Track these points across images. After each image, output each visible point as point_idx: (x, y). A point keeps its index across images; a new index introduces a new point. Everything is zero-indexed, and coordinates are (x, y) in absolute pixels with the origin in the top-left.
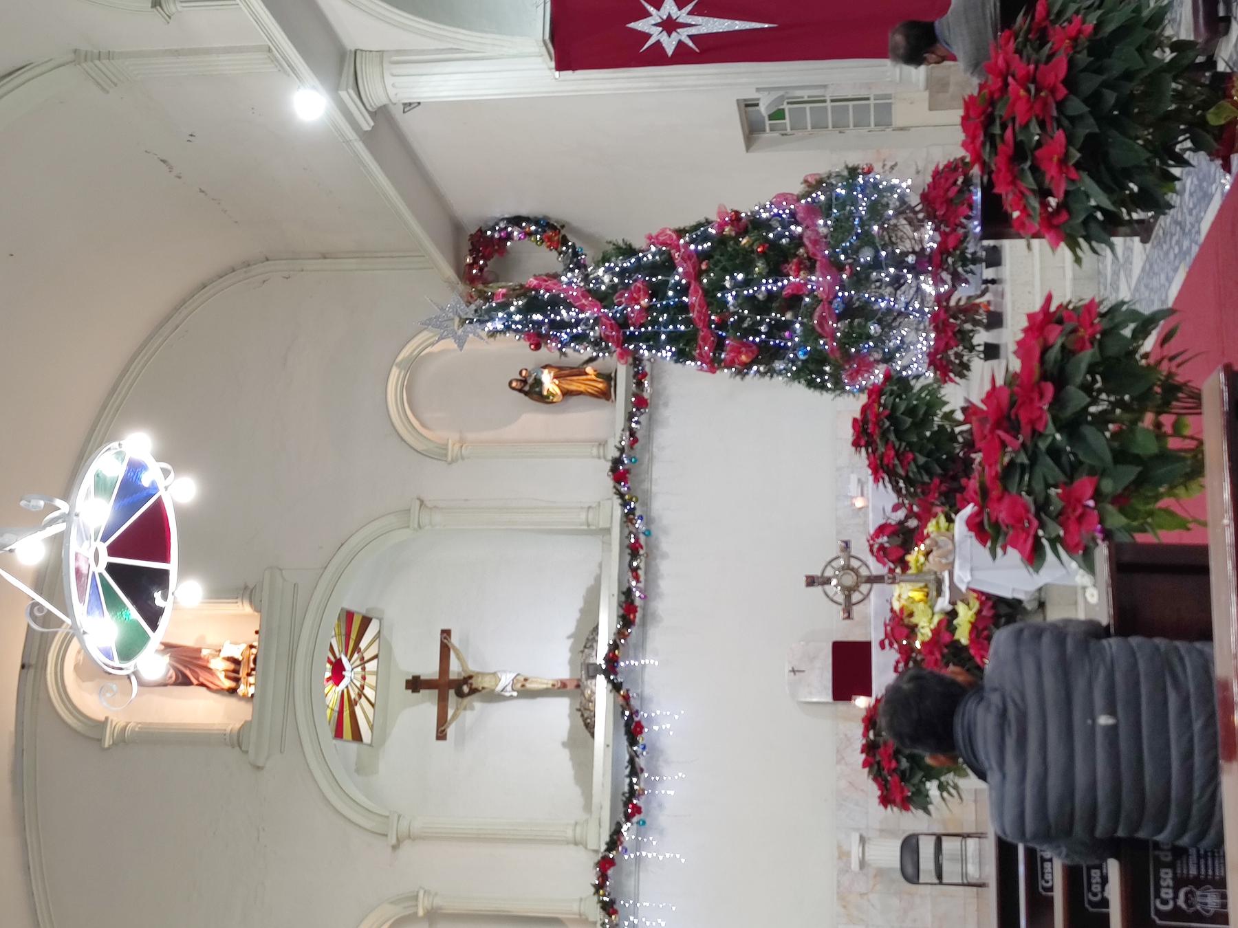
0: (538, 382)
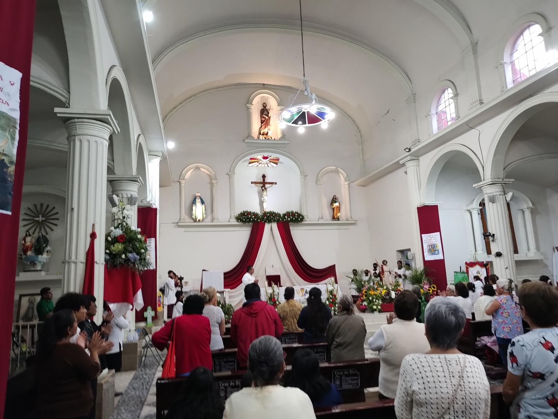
0: (336, 202)
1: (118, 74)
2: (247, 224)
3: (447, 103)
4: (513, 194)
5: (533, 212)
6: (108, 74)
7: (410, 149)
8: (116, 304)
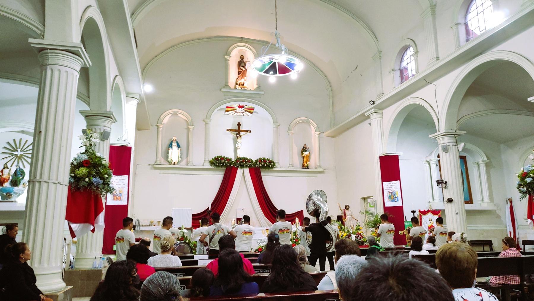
0: (306, 151)
1: (95, 14)
2: (220, 168)
3: (409, 61)
4: (465, 145)
5: (488, 165)
6: (84, 12)
7: (374, 102)
8: (78, 224)
